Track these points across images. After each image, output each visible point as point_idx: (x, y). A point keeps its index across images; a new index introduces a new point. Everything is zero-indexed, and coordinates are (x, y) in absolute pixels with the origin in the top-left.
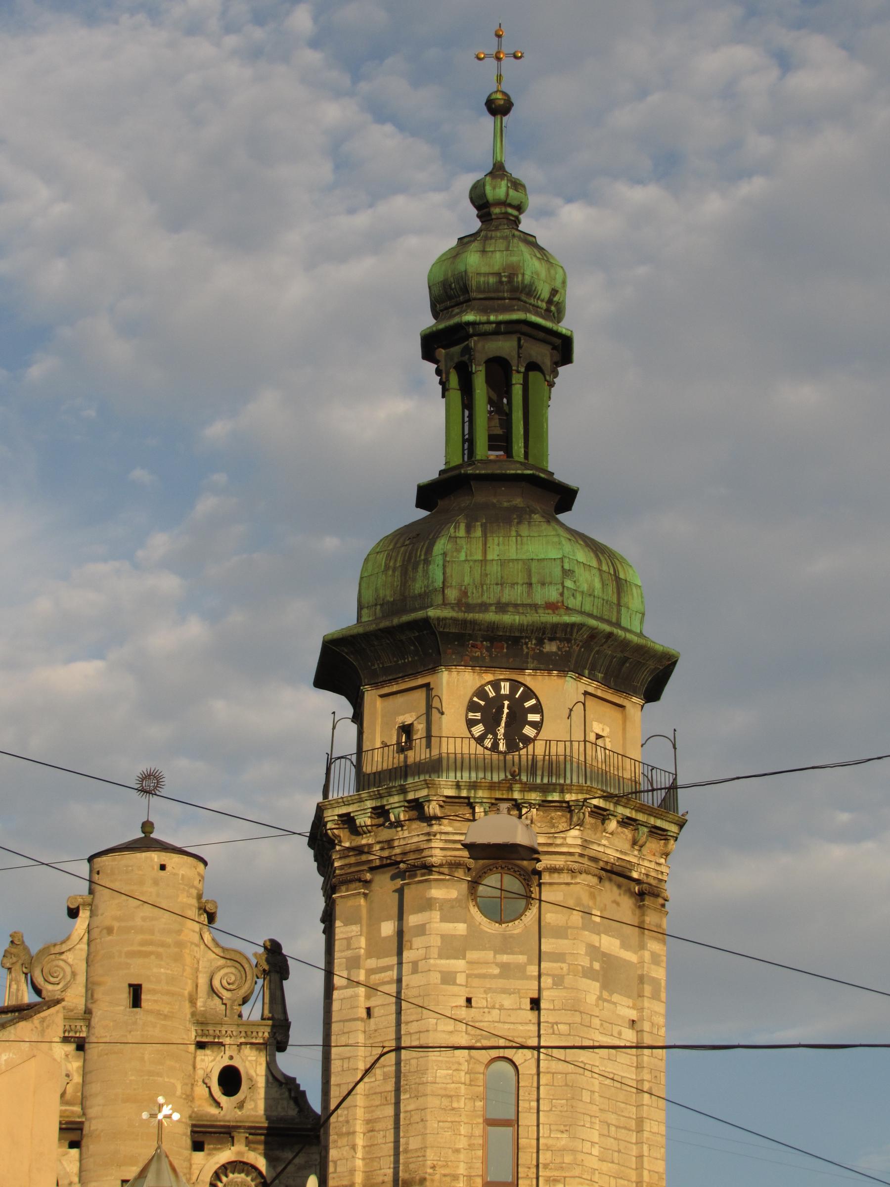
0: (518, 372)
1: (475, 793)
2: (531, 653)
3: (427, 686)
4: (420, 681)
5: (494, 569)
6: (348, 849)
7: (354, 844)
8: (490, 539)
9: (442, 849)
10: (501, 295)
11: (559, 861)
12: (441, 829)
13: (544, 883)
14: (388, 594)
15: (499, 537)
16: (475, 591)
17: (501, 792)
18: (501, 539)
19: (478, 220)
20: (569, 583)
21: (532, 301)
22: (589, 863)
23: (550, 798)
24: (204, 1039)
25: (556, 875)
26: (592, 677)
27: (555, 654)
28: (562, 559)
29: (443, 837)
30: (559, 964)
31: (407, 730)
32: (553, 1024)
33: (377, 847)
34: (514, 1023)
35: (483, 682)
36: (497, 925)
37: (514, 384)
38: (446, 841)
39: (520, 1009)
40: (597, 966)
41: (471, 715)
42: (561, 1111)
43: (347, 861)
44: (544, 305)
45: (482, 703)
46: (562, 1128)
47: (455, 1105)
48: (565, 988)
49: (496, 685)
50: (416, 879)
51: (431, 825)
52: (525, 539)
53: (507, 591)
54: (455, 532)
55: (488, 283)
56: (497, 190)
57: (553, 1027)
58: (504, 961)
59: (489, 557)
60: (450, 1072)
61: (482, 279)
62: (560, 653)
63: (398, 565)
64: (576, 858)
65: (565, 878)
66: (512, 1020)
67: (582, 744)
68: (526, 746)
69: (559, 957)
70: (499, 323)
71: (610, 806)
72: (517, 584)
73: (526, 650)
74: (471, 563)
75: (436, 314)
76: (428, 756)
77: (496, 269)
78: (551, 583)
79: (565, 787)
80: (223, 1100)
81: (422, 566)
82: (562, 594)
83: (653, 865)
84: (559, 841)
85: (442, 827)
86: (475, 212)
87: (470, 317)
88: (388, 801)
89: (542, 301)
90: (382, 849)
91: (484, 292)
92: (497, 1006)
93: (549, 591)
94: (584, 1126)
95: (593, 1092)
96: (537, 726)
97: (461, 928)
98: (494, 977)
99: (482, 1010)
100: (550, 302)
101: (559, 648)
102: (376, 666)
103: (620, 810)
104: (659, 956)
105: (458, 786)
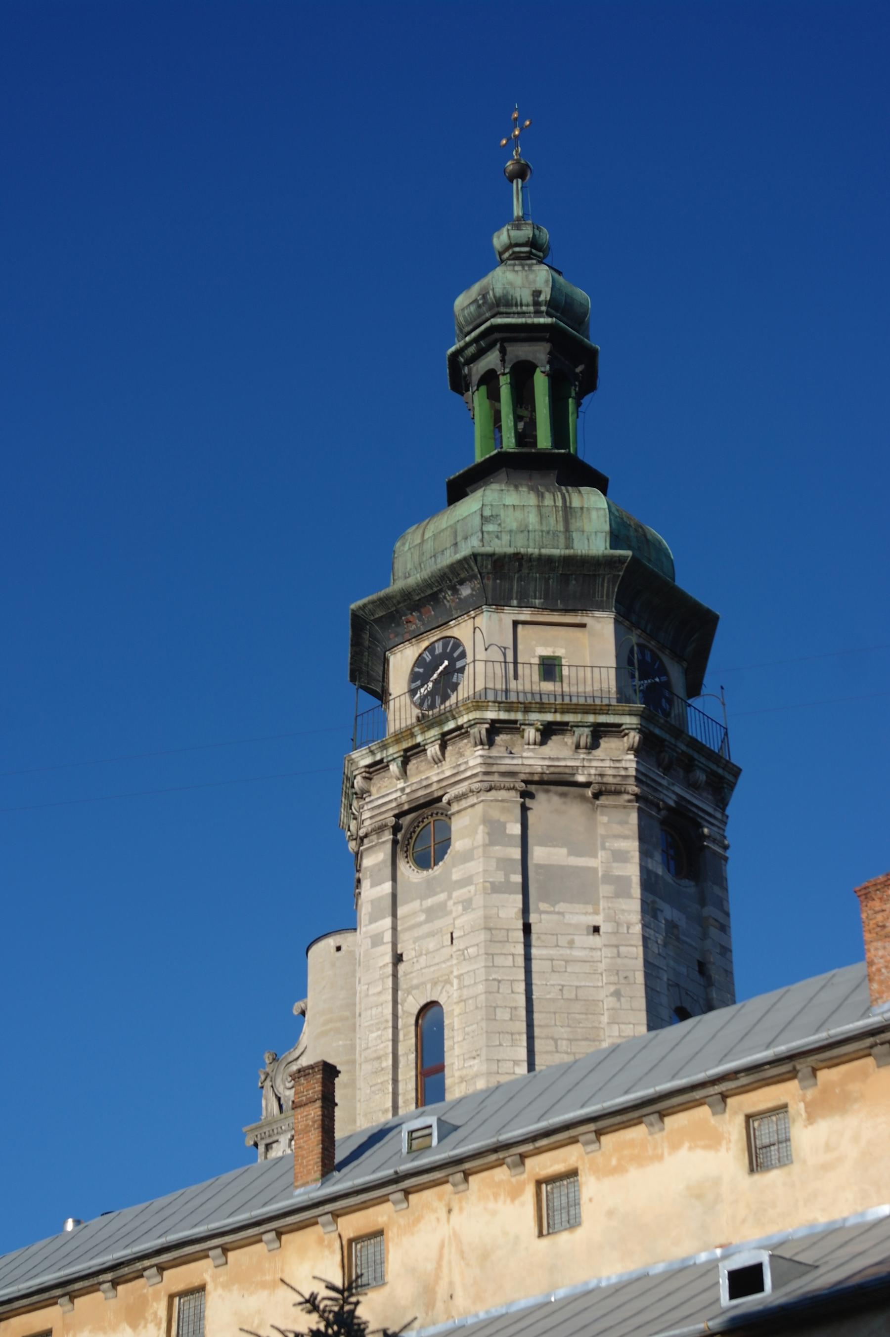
0: (504, 374)
2: (453, 605)
9: (371, 818)
10: (484, 317)
13: (453, 814)
17: (407, 742)
21: (514, 309)
22: (501, 779)
27: (471, 595)
29: (370, 806)
32: (463, 951)
34: (438, 964)
35: (420, 651)
38: (373, 808)
39: (443, 947)
42: (473, 1037)
44: (531, 309)
47: (384, 1064)
53: (439, 560)
55: (471, 313)
57: (463, 954)
60: (379, 1032)
61: (466, 312)
62: (474, 593)
66: (437, 960)
69: (467, 881)
71: (519, 716)
72: (446, 549)
73: (448, 604)
78: (472, 534)
79: (454, 713)
84: (462, 768)
89: (528, 305)
91: (472, 322)
92: (424, 952)
94: (500, 1045)
98: (419, 925)
99: (411, 962)
101: (473, 589)
103: (534, 717)
104: (627, 852)
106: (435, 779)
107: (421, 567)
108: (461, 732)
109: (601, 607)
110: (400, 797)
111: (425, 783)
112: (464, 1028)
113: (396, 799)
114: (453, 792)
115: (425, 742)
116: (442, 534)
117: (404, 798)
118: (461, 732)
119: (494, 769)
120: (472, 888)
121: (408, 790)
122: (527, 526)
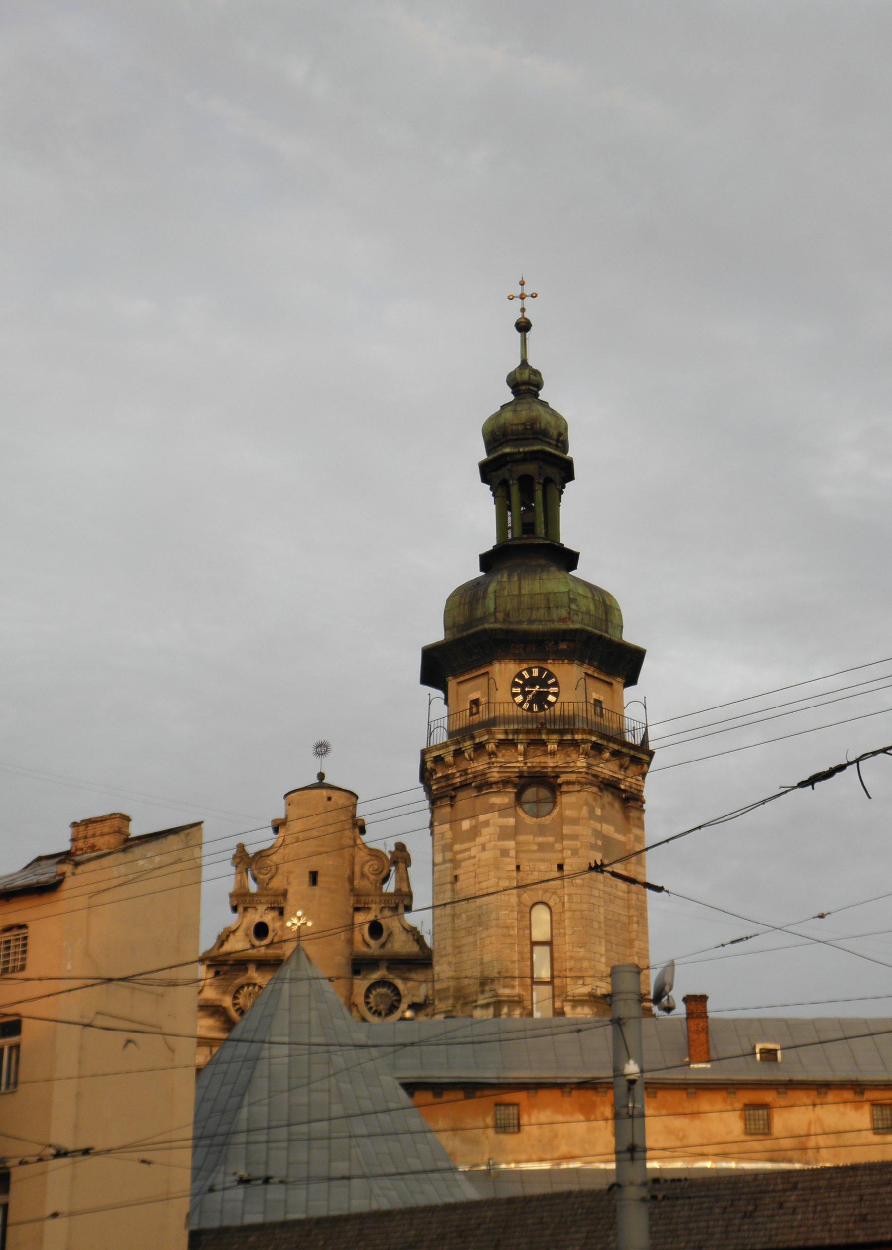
0: (539, 483)
1: (517, 736)
3: (487, 673)
4: (482, 671)
5: (526, 599)
6: (441, 777)
7: (444, 774)
8: (523, 582)
9: (498, 772)
10: (527, 436)
11: (573, 777)
12: (497, 760)
14: (461, 620)
15: (528, 581)
16: (514, 614)
18: (530, 581)
19: (512, 395)
20: (573, 607)
21: (546, 440)
22: (593, 779)
23: (565, 738)
24: (359, 906)
25: (571, 786)
26: (590, 664)
28: (568, 592)
30: (575, 842)
31: (476, 702)
33: (458, 775)
35: (521, 669)
36: (535, 819)
37: (537, 490)
40: (599, 843)
41: (514, 690)
43: (440, 785)
45: (521, 682)
46: (580, 945)
47: (512, 933)
48: (579, 857)
49: (530, 671)
50: (482, 793)
51: (490, 758)
52: (545, 581)
53: (534, 613)
54: (501, 578)
56: (523, 376)
58: (540, 841)
59: (523, 592)
60: (507, 912)
63: (467, 601)
64: (584, 775)
65: (577, 787)
67: (585, 703)
68: (549, 707)
69: (574, 837)
70: (525, 453)
71: (605, 743)
72: (541, 608)
73: (547, 648)
74: (512, 597)
75: (489, 451)
76: (487, 717)
77: (523, 420)
78: (562, 607)
79: (574, 731)
80: (372, 942)
81: (481, 601)
82: (569, 613)
83: (634, 781)
84: (572, 765)
85: (498, 759)
86: (510, 390)
87: (508, 450)
88: (463, 745)
89: (553, 440)
90: (461, 776)
92: (536, 870)
93: (561, 612)
94: (595, 944)
95: (600, 922)
96: (556, 694)
97: (511, 821)
98: (534, 851)
100: (558, 440)
101: (568, 646)
102: (455, 664)
105: (506, 732)
106: (551, 765)
107: (519, 611)
108: (575, 744)
109: (619, 676)
110: (522, 767)
111: (542, 765)
112: (573, 928)
113: (519, 767)
114: (563, 778)
115: (548, 740)
116: (537, 596)
117: (525, 769)
118: (575, 744)
119: (590, 772)
120: (579, 843)
121: (529, 765)
122: (590, 612)
